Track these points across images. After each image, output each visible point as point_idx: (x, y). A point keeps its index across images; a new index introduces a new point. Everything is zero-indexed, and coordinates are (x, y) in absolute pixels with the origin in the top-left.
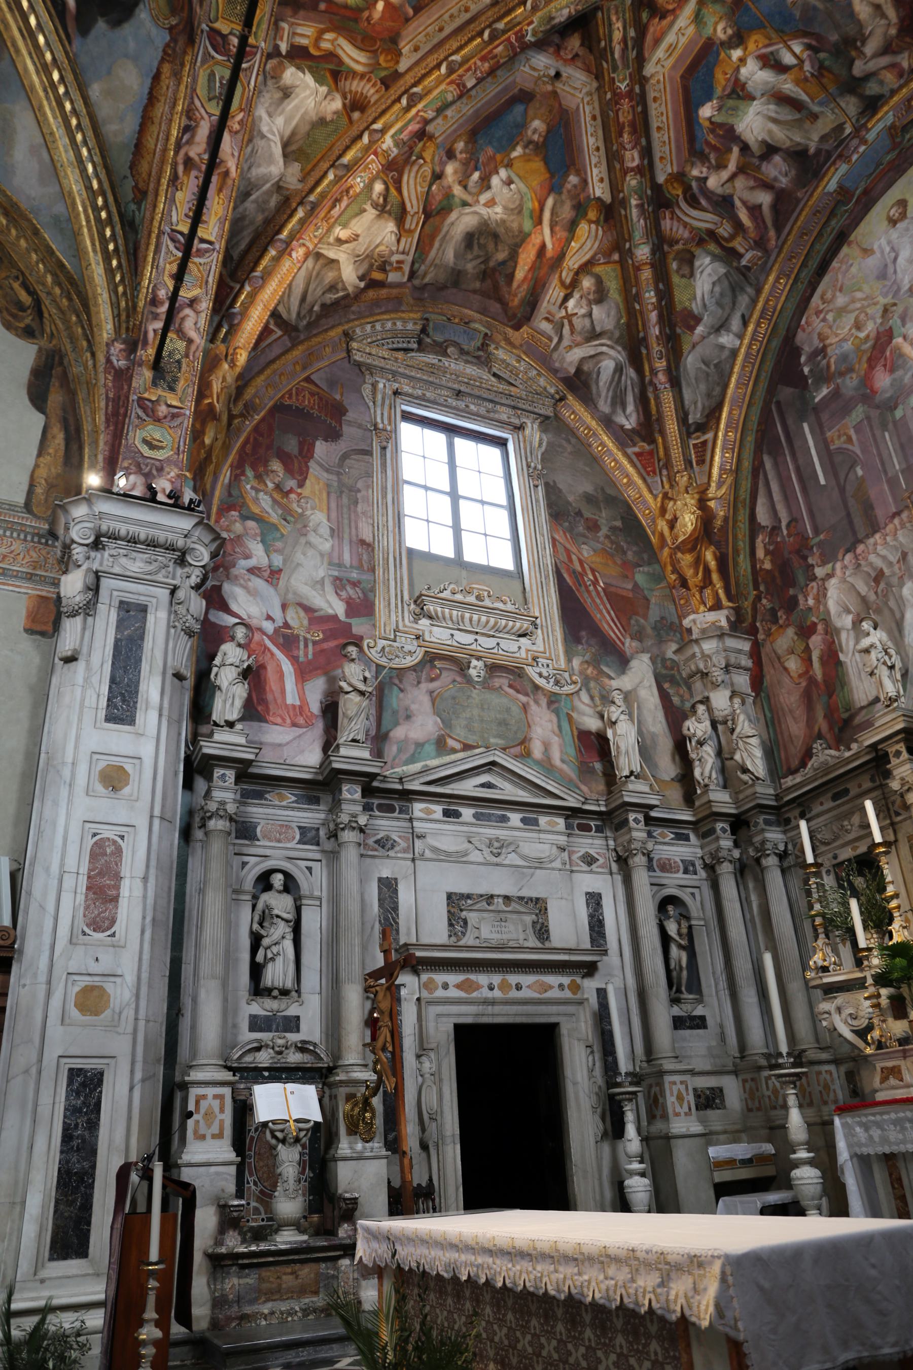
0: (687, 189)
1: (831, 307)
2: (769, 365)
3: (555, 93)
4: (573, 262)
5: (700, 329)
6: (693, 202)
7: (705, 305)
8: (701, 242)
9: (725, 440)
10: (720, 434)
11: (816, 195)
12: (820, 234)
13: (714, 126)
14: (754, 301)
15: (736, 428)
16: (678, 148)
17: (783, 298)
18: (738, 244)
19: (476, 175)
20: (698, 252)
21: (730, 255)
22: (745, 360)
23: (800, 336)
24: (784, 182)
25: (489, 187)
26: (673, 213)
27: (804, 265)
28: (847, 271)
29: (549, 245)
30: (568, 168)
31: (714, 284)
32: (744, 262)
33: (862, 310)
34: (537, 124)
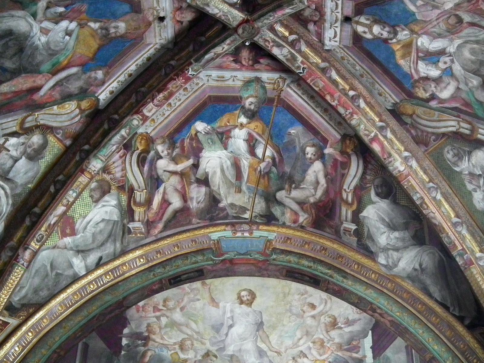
0: (146, 151)
1: (168, 314)
2: (95, 309)
3: (149, 24)
4: (43, 117)
5: (68, 240)
6: (141, 162)
7: (85, 228)
8: (121, 188)
9: (23, 336)
10: (24, 328)
11: (202, 231)
12: (185, 256)
13: (195, 138)
14: (116, 257)
15: (38, 333)
16: (167, 126)
17: (134, 272)
18: (139, 211)
19: (61, 9)
20: (114, 191)
21: (128, 213)
22: (78, 290)
23: (132, 313)
24: (193, 205)
25: (57, 23)
26: (125, 155)
27: (162, 264)
28: (193, 301)
29: (42, 92)
30: (105, 66)
31: (103, 220)
32: (131, 225)
33: (190, 338)
34: (122, 26)
